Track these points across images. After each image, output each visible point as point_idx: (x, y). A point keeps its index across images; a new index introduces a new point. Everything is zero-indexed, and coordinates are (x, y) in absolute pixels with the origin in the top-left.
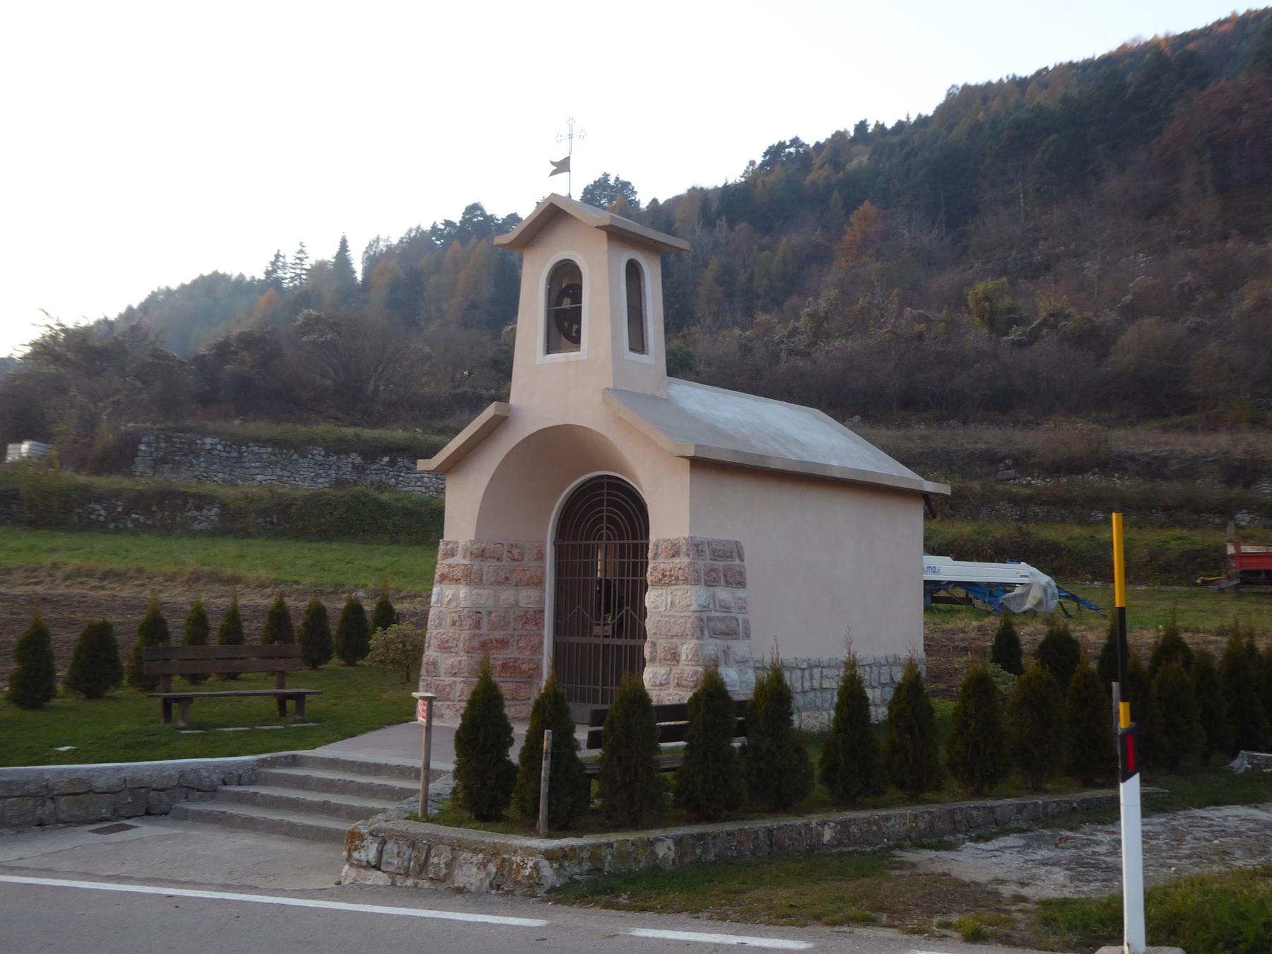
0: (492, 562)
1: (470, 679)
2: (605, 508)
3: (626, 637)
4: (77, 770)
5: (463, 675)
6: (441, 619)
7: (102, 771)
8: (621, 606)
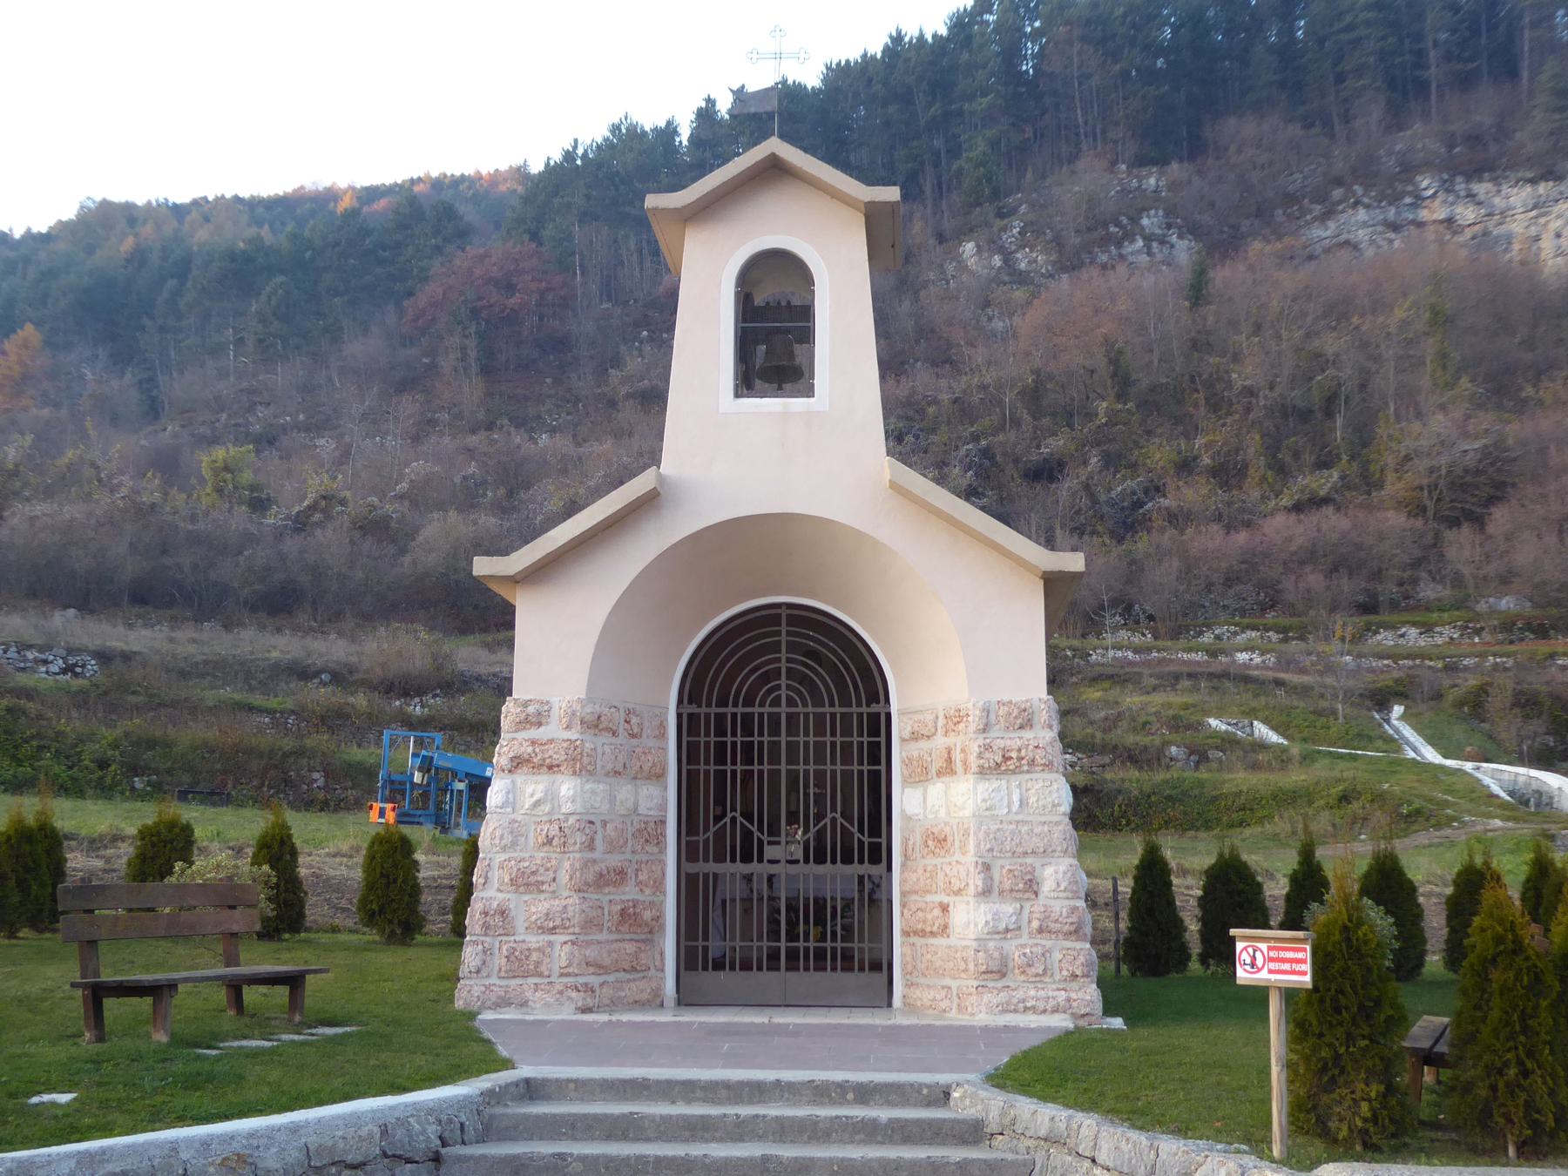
0: (606, 738)
1: (581, 938)
2: (783, 655)
3: (834, 861)
4: (232, 1137)
5: (571, 930)
6: (516, 833)
7: (270, 1133)
8: (819, 817)
